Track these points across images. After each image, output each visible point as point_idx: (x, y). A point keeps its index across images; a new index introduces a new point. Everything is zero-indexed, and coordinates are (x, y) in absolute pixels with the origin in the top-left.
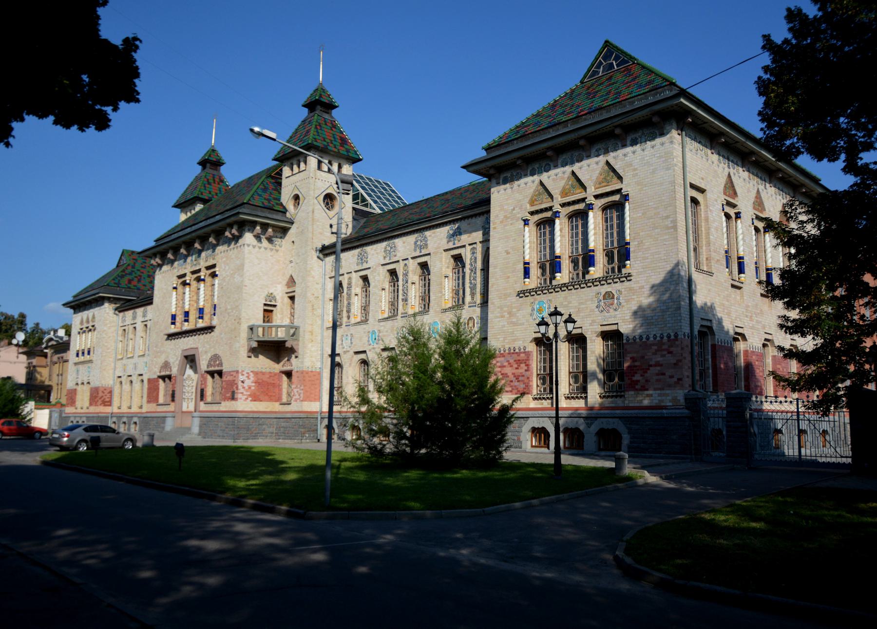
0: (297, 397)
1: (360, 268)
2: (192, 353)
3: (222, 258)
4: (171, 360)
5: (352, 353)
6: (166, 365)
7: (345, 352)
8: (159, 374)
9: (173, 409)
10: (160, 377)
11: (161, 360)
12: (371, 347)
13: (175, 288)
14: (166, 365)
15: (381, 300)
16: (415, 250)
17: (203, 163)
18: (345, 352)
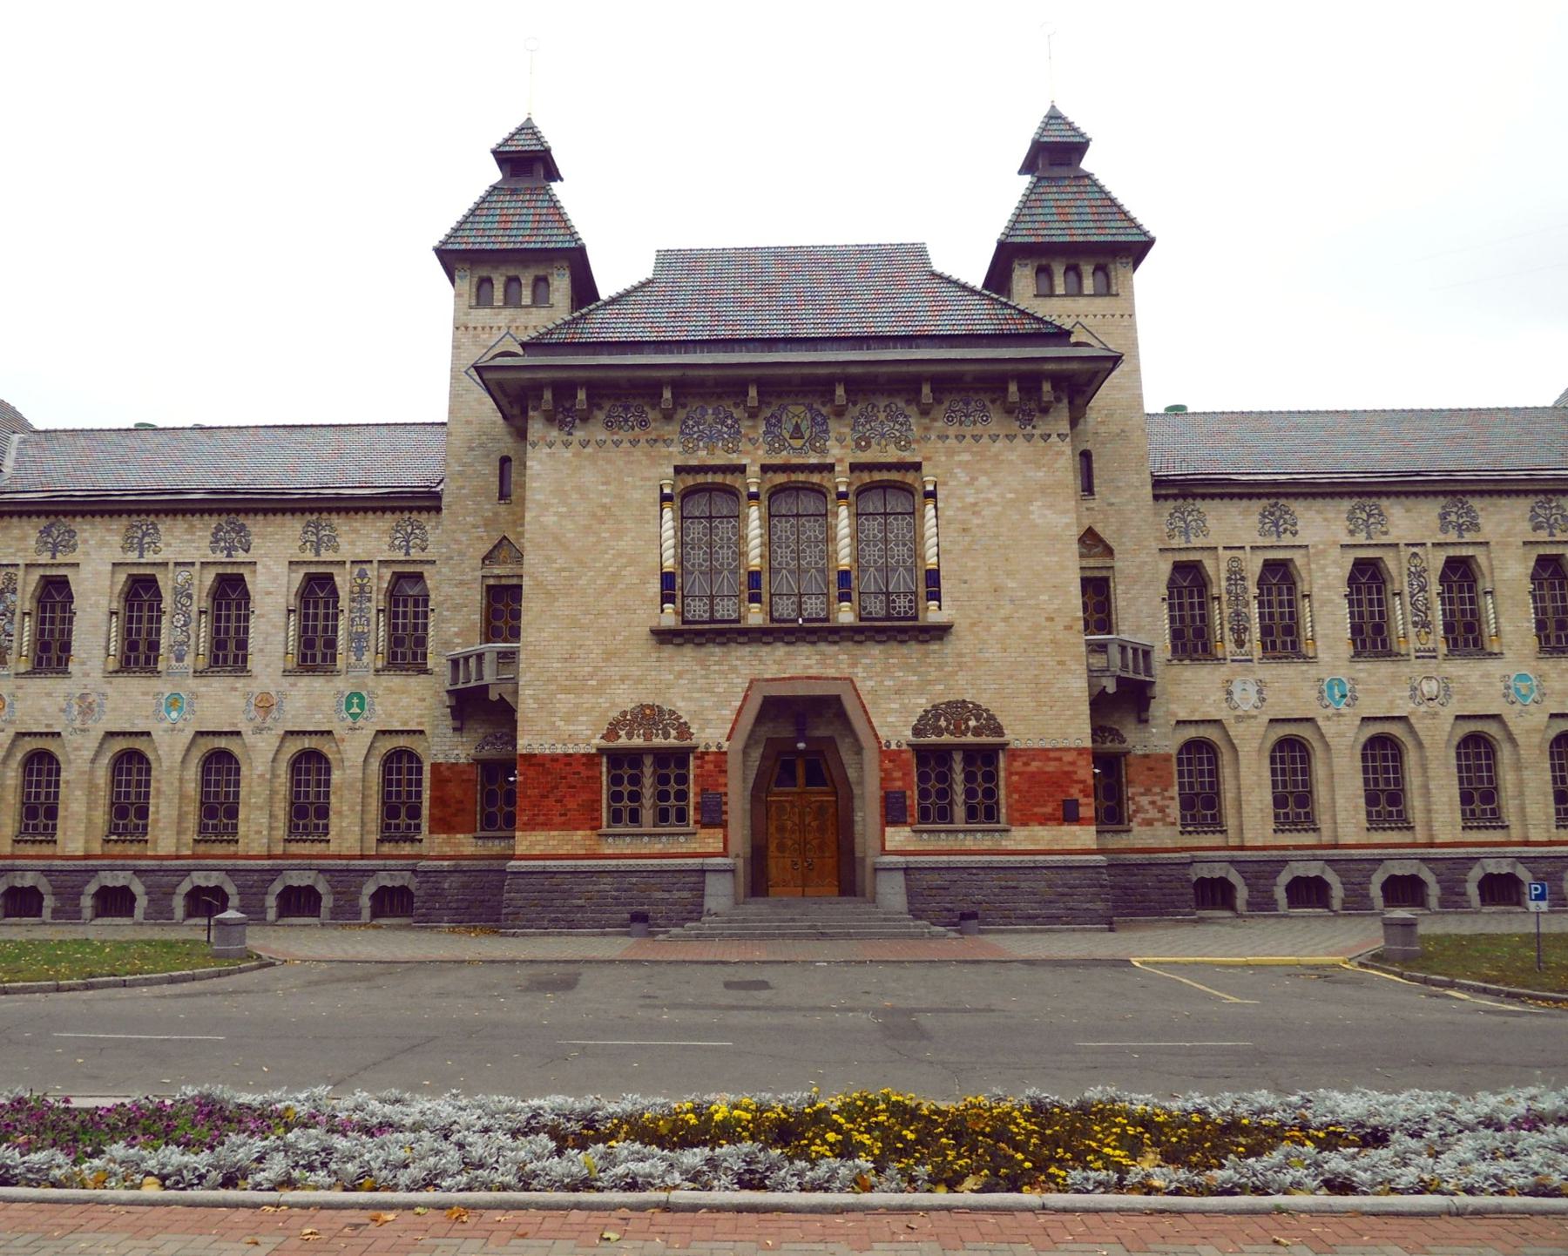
0: (1153, 813)
1: (1272, 540)
3: (951, 453)
4: (684, 708)
5: (1266, 719)
7: (1239, 719)
8: (597, 741)
9: (718, 846)
10: (601, 751)
12: (1330, 711)
13: (665, 498)
14: (649, 717)
15: (1328, 615)
16: (1444, 529)
17: (503, 157)
18: (1239, 719)
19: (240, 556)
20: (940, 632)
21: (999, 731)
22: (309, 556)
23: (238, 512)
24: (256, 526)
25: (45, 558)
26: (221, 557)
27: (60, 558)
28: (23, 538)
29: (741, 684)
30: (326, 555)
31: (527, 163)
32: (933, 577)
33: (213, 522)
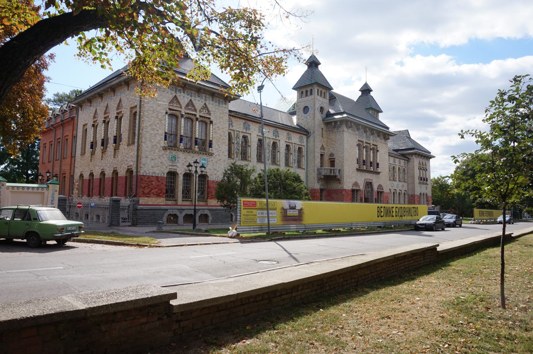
2: (370, 181)
4: (359, 182)
6: (356, 184)
11: (354, 180)
14: (356, 184)
19: (278, 138)
20: (379, 173)
21: (383, 189)
22: (288, 141)
23: (277, 127)
24: (280, 131)
25: (244, 131)
26: (274, 137)
27: (247, 132)
28: (240, 125)
29: (363, 179)
30: (290, 141)
31: (313, 64)
32: (378, 164)
33: (273, 129)
